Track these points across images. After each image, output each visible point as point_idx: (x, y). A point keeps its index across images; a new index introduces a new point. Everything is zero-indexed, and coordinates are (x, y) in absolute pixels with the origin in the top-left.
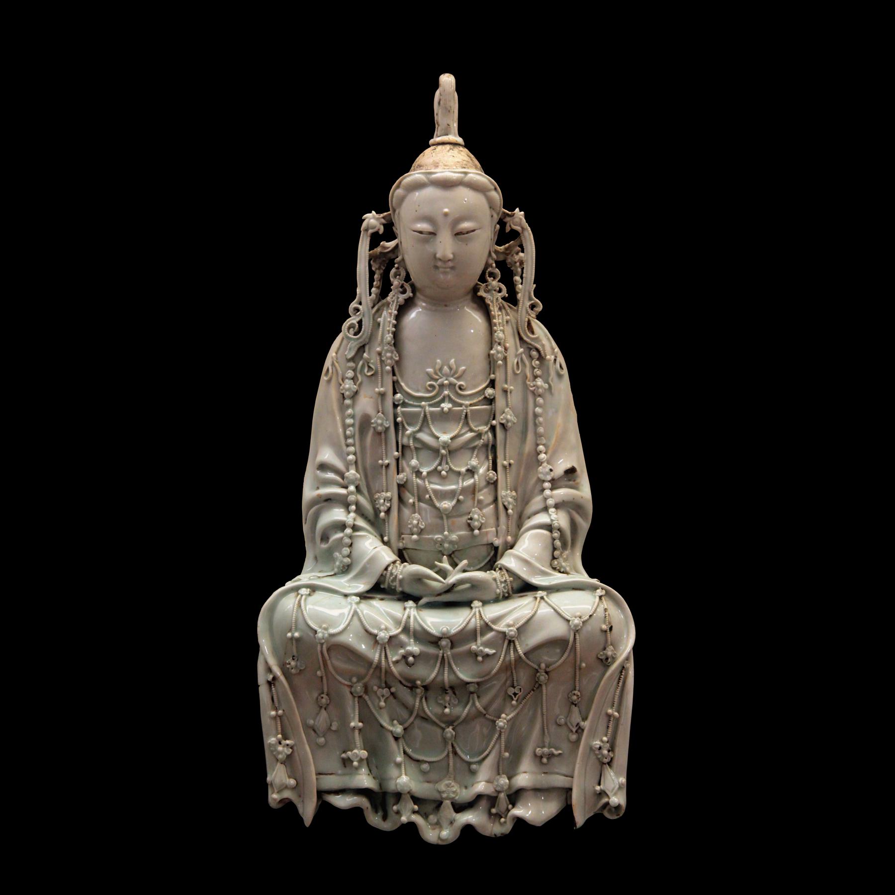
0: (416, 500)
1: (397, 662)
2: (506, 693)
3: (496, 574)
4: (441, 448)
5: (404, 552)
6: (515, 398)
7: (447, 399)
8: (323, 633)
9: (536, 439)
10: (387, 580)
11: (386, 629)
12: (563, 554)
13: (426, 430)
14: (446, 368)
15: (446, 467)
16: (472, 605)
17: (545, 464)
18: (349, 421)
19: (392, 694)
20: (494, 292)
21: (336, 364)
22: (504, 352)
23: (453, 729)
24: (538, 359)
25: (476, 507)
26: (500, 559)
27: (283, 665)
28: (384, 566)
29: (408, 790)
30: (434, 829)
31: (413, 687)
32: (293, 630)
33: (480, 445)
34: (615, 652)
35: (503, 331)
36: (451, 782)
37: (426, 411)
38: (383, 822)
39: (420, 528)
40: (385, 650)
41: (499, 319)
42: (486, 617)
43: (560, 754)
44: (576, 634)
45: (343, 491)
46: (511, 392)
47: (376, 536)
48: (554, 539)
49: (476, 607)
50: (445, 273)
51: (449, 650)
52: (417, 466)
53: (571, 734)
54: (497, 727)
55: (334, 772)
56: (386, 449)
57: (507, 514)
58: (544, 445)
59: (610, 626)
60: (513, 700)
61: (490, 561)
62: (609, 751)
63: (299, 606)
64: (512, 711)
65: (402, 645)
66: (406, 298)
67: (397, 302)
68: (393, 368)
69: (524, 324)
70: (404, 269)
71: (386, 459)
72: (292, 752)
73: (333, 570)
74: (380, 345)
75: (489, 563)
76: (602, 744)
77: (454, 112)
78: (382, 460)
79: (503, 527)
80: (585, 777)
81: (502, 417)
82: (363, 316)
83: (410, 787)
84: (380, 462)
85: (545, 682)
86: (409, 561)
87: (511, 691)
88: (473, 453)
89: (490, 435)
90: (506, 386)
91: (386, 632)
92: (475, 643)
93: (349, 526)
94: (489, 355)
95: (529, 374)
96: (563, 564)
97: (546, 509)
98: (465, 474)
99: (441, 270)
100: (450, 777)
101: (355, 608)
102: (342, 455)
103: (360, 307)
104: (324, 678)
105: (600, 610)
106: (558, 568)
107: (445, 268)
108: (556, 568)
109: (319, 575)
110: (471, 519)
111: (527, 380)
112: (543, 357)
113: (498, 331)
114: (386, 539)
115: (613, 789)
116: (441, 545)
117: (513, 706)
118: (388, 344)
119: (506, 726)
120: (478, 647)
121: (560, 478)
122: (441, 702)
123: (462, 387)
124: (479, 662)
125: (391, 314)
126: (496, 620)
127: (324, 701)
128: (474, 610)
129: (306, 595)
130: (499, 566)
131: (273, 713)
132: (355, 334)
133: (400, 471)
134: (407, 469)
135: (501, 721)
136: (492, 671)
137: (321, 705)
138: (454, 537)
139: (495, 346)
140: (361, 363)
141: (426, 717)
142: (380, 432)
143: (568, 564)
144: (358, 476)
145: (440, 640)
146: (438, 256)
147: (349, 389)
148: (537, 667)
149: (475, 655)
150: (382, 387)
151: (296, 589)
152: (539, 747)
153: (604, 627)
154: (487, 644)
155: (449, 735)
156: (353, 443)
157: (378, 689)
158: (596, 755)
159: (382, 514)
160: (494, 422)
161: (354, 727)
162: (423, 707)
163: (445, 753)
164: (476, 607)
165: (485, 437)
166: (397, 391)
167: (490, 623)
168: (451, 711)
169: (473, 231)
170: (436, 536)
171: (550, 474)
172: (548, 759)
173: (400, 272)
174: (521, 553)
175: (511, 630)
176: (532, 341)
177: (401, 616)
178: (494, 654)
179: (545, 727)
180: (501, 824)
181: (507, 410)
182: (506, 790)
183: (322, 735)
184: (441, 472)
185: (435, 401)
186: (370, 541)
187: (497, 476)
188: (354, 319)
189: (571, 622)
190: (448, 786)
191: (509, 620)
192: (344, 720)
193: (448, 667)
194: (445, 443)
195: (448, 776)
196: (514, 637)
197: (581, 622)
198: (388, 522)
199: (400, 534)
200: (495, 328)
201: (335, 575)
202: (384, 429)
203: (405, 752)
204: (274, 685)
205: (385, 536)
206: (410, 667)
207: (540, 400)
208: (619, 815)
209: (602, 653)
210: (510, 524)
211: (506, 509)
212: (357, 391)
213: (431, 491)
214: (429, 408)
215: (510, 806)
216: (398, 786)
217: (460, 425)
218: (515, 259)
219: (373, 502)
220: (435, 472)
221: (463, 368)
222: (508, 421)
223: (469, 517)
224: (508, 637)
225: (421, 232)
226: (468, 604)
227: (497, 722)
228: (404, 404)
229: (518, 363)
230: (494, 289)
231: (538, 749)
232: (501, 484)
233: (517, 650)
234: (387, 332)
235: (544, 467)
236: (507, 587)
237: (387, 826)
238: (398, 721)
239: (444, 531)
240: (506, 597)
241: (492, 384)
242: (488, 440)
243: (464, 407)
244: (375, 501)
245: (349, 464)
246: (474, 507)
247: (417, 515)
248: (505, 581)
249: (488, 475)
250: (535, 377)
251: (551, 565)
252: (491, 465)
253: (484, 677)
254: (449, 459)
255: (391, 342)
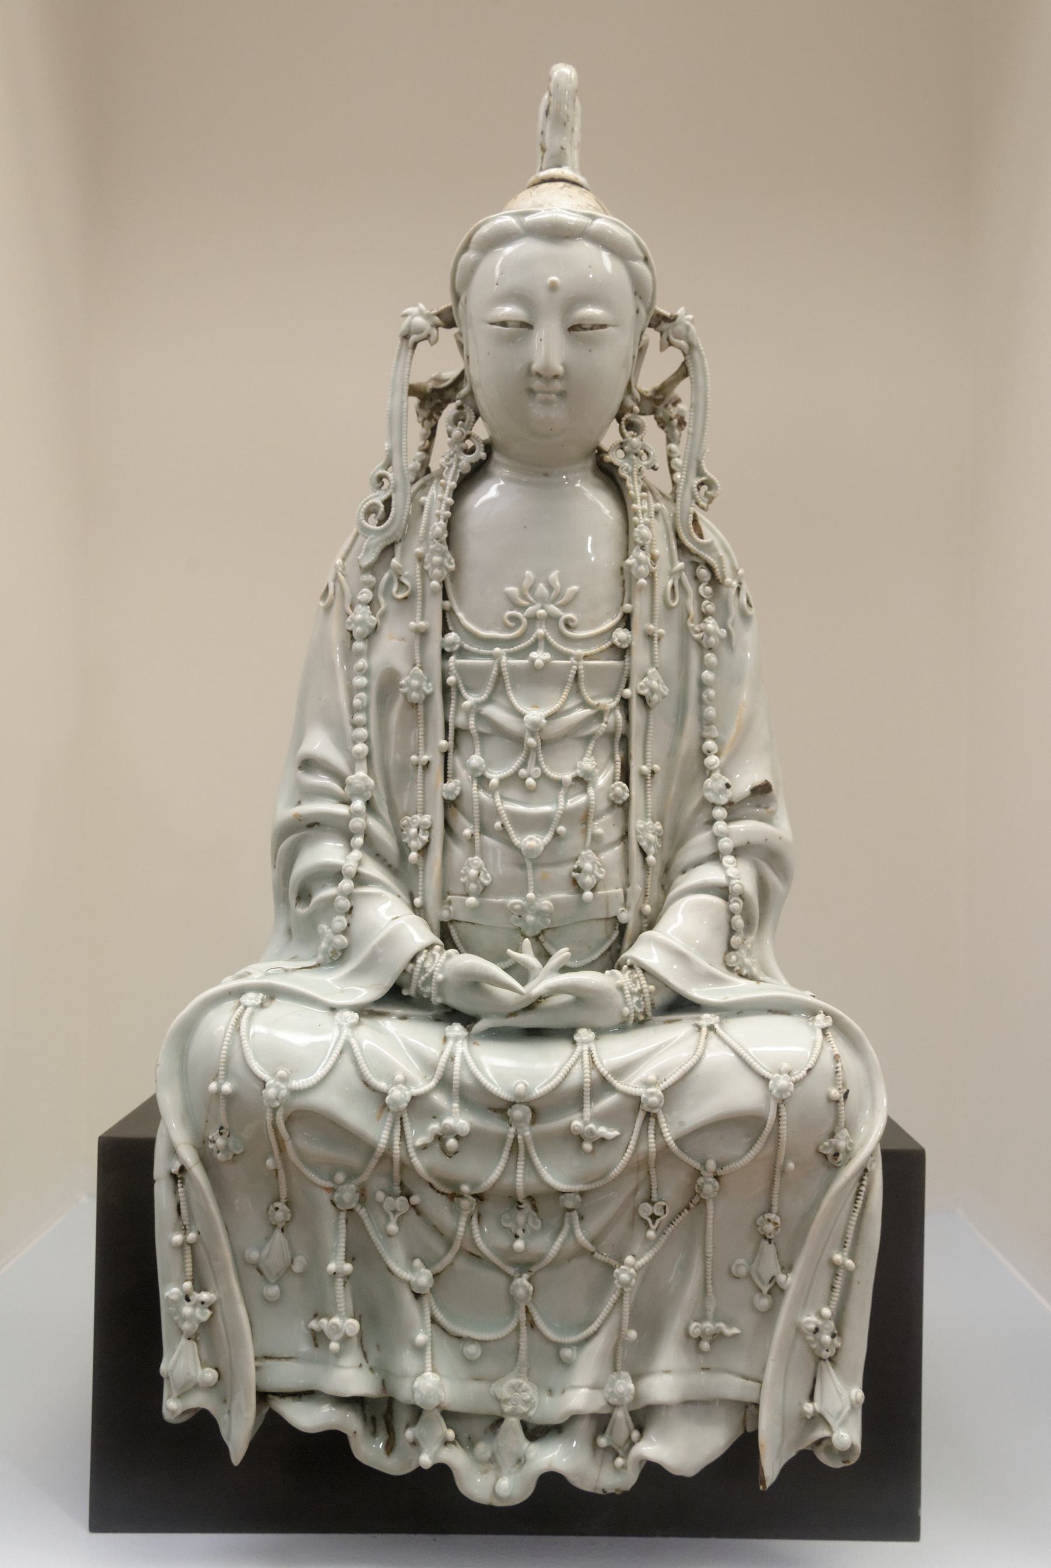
0: (477, 830)
1: (425, 1147)
2: (636, 1211)
3: (622, 977)
4: (527, 734)
5: (451, 927)
6: (667, 650)
7: (542, 644)
8: (278, 1088)
9: (702, 729)
10: (414, 981)
11: (406, 1082)
12: (745, 942)
13: (500, 699)
14: (542, 588)
15: (535, 770)
16: (576, 1038)
17: (717, 774)
18: (360, 681)
19: (414, 1207)
20: (635, 457)
21: (342, 577)
22: (650, 565)
23: (529, 1280)
24: (710, 584)
25: (590, 848)
26: (630, 946)
27: (204, 1142)
28: (409, 955)
29: (436, 1403)
30: (486, 1472)
31: (454, 1195)
32: (220, 1077)
33: (599, 732)
34: (851, 1141)
35: (648, 525)
36: (520, 1381)
37: (502, 665)
38: (385, 1456)
39: (482, 883)
40: (402, 1124)
41: (642, 505)
42: (602, 1063)
43: (735, 1336)
44: (782, 1106)
45: (342, 810)
46: (659, 640)
47: (399, 896)
48: (731, 914)
49: (584, 1042)
50: (547, 403)
51: (527, 1128)
52: (481, 766)
53: (757, 1296)
54: (616, 1282)
55: (293, 1355)
56: (425, 735)
57: (645, 862)
58: (714, 739)
59: (845, 1091)
60: (649, 1228)
61: (609, 949)
62: (833, 1336)
63: (237, 1029)
64: (648, 1250)
65: (436, 1114)
66: (474, 461)
67: (457, 467)
68: (444, 583)
69: (688, 517)
70: (473, 413)
71: (426, 752)
72: (212, 1316)
73: (316, 956)
74: (421, 542)
75: (609, 953)
76: (820, 1322)
77: (573, 130)
78: (418, 755)
79: (637, 887)
80: (785, 1386)
81: (642, 683)
82: (395, 490)
83: (440, 1397)
84: (414, 757)
85: (712, 1196)
86: (459, 945)
87: (645, 1210)
88: (586, 749)
89: (619, 715)
90: (651, 626)
91: (404, 1087)
92: (579, 1115)
93: (348, 876)
94: (622, 569)
95: (693, 610)
96: (747, 960)
97: (716, 857)
98: (571, 786)
99: (540, 396)
100: (520, 1372)
101: (347, 1036)
102: (343, 743)
103: (389, 473)
104: (281, 1173)
105: (827, 1061)
106: (738, 968)
107: (549, 393)
108: (734, 967)
109: (286, 967)
110: (579, 870)
111: (690, 619)
112: (718, 580)
113: (640, 523)
114: (418, 901)
115: (840, 1413)
116: (520, 916)
117: (647, 1240)
118: (437, 539)
119: (634, 1280)
120: (586, 1124)
121: (743, 801)
122: (509, 1225)
123: (571, 624)
124: (586, 1153)
125: (444, 486)
126: (621, 1071)
127: (279, 1215)
128: (579, 1048)
129: (255, 1007)
130: (629, 961)
131: (177, 1238)
132: (380, 523)
133: (448, 776)
134: (463, 773)
135: (624, 1271)
136: (610, 1171)
137: (274, 1223)
138: (545, 903)
139: (634, 551)
140: (386, 576)
141: (478, 1254)
142: (415, 702)
143: (755, 961)
144: (371, 782)
145: (511, 1107)
146: (535, 367)
147: (361, 623)
148: (698, 1166)
149: (580, 1139)
150: (423, 618)
151: (237, 993)
152: (695, 1321)
153: (835, 1093)
154: (603, 1118)
155: (521, 1292)
156: (365, 722)
157: (386, 1197)
158: (808, 1342)
159: (413, 855)
160: (627, 692)
161: (335, 1273)
162: (472, 1235)
163: (513, 1325)
164: (584, 1042)
165: (609, 719)
166: (451, 628)
167: (610, 1076)
168: (526, 1245)
169: (603, 326)
170: (513, 901)
171: (725, 793)
172: (711, 1343)
173: (464, 415)
174: (671, 938)
175: (652, 1094)
176: (700, 549)
177: (438, 1054)
178: (616, 1138)
179: (709, 1282)
180: (616, 1470)
181: (652, 671)
182: (629, 1405)
183: (274, 1281)
184: (525, 779)
185: (519, 646)
186: (389, 904)
187: (629, 793)
188: (377, 496)
189: (771, 1082)
190: (514, 1388)
191: (647, 1071)
192: (317, 1257)
193: (525, 1161)
194: (535, 725)
195: (516, 1370)
196: (656, 1108)
197: (792, 1083)
198: (423, 870)
199: (445, 894)
200: (636, 518)
201: (318, 965)
202: (423, 697)
203: (434, 1320)
204: (182, 1179)
205: (418, 896)
206: (450, 1157)
207: (711, 657)
208: (848, 1461)
209: (826, 1143)
210: (649, 883)
211: (644, 854)
212: (377, 626)
213: (505, 815)
214: (508, 659)
215: (635, 1434)
216: (417, 1396)
217: (564, 696)
218: (671, 413)
219: (398, 832)
220: (515, 780)
221: (575, 588)
222: (653, 691)
223: (576, 866)
224: (644, 1106)
225: (504, 324)
226: (567, 1033)
227: (617, 1271)
228: (462, 652)
229: (673, 587)
230: (635, 451)
231: (694, 1324)
232: (635, 808)
233: (662, 1134)
234: (437, 518)
235: (715, 780)
236: (642, 1003)
237: (393, 1465)
238: (423, 1261)
239: (528, 892)
240: (641, 1023)
241: (627, 621)
242: (616, 726)
243: (573, 660)
244: (402, 830)
245: (355, 759)
246: (585, 849)
247: (477, 859)
248: (641, 992)
249: (613, 789)
250: (704, 615)
251: (725, 962)
252: (619, 771)
253: (595, 1181)
254: (541, 755)
255: (443, 535)
